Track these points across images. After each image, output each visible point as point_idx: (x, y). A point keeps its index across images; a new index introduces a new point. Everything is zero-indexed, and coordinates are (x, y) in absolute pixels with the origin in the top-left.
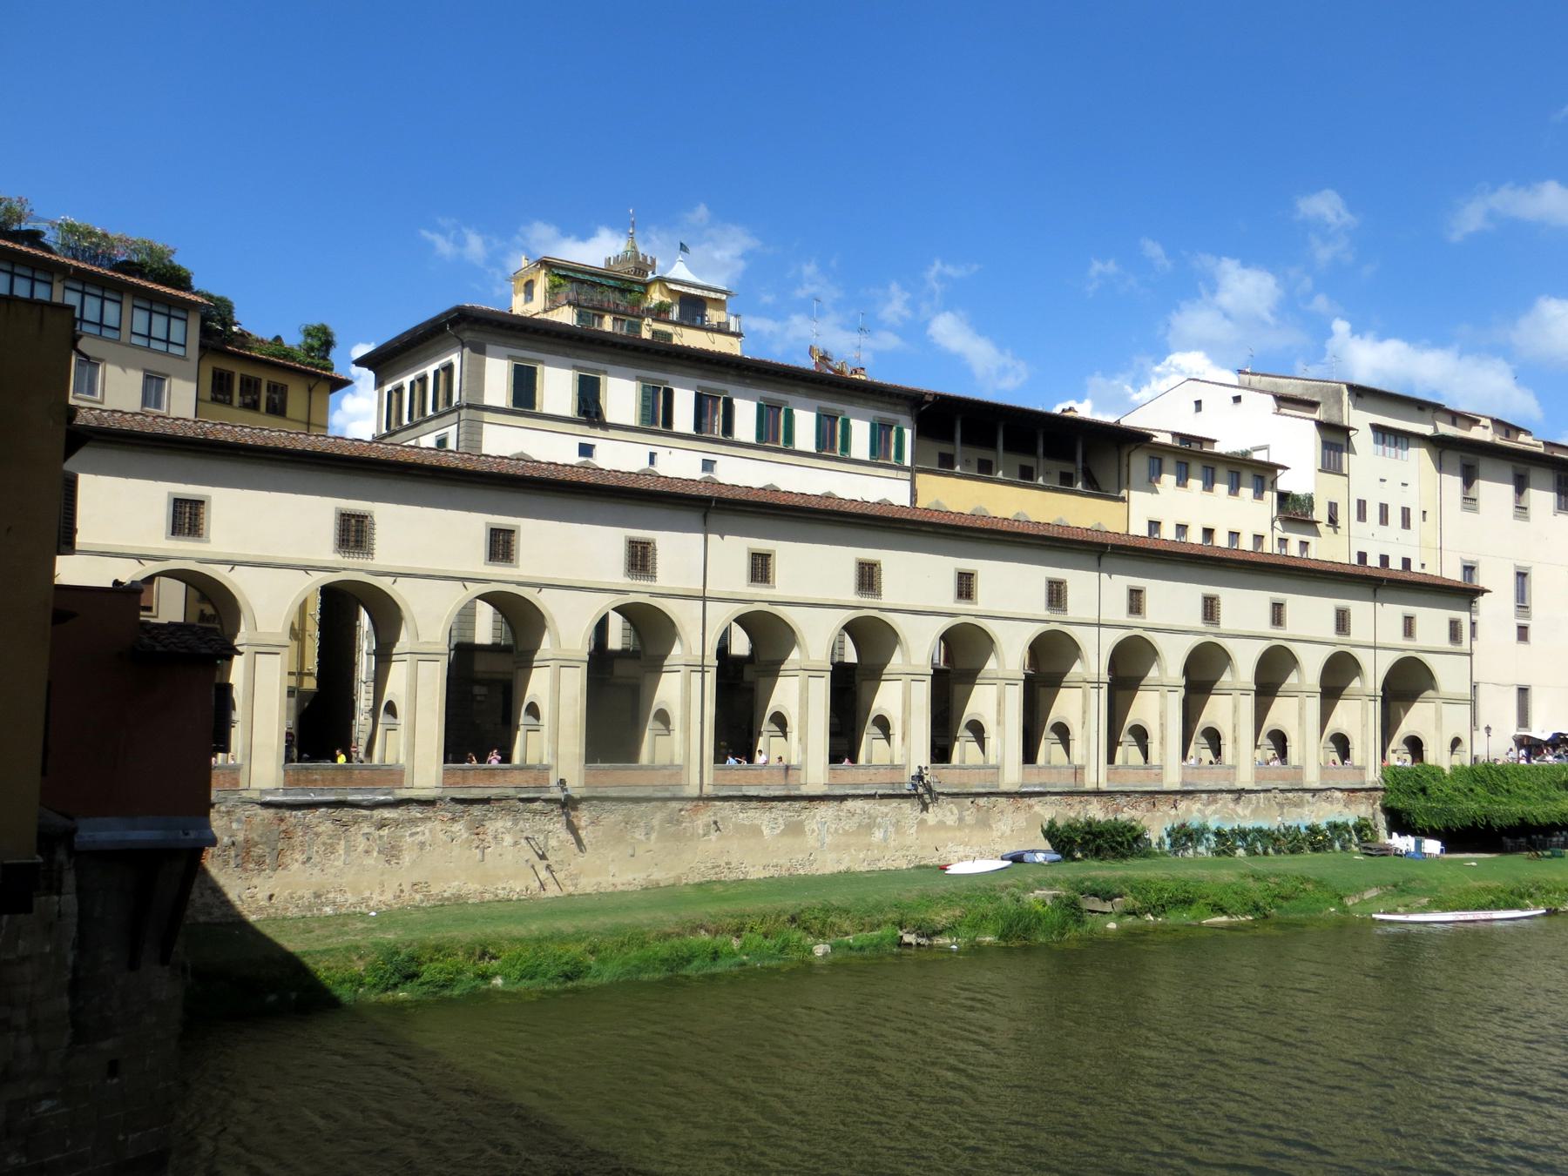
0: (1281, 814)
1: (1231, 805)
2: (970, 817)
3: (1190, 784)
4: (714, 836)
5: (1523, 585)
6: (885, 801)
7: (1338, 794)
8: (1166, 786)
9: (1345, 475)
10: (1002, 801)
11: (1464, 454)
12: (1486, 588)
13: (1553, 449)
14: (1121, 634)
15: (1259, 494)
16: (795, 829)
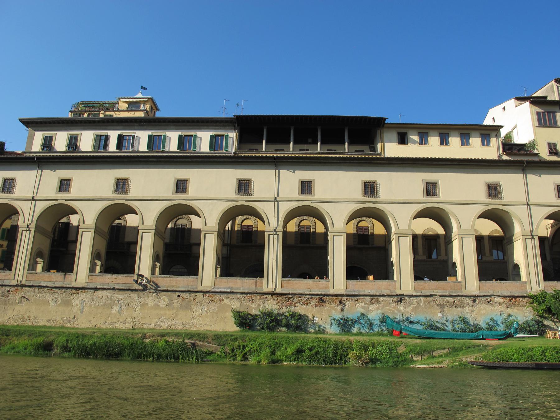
2: (176, 304)
3: (354, 291)
4: (25, 302)
6: (121, 292)
10: (200, 295)
16: (68, 303)
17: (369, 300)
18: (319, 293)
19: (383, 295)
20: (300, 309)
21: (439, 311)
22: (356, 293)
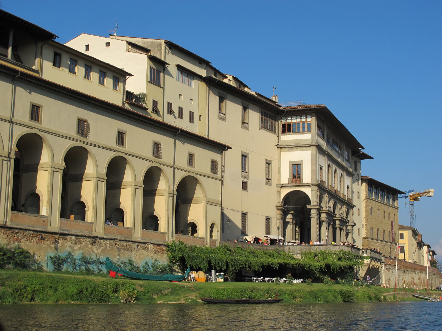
0: (119, 255)
1: (90, 246)
3: (65, 230)
5: (245, 161)
7: (151, 246)
8: (49, 229)
9: (162, 88)
11: (221, 91)
12: (230, 146)
14: (25, 131)
15: (115, 88)
17: (75, 239)
18: (41, 229)
19: (85, 236)
20: (25, 245)
21: (117, 254)
22: (66, 232)
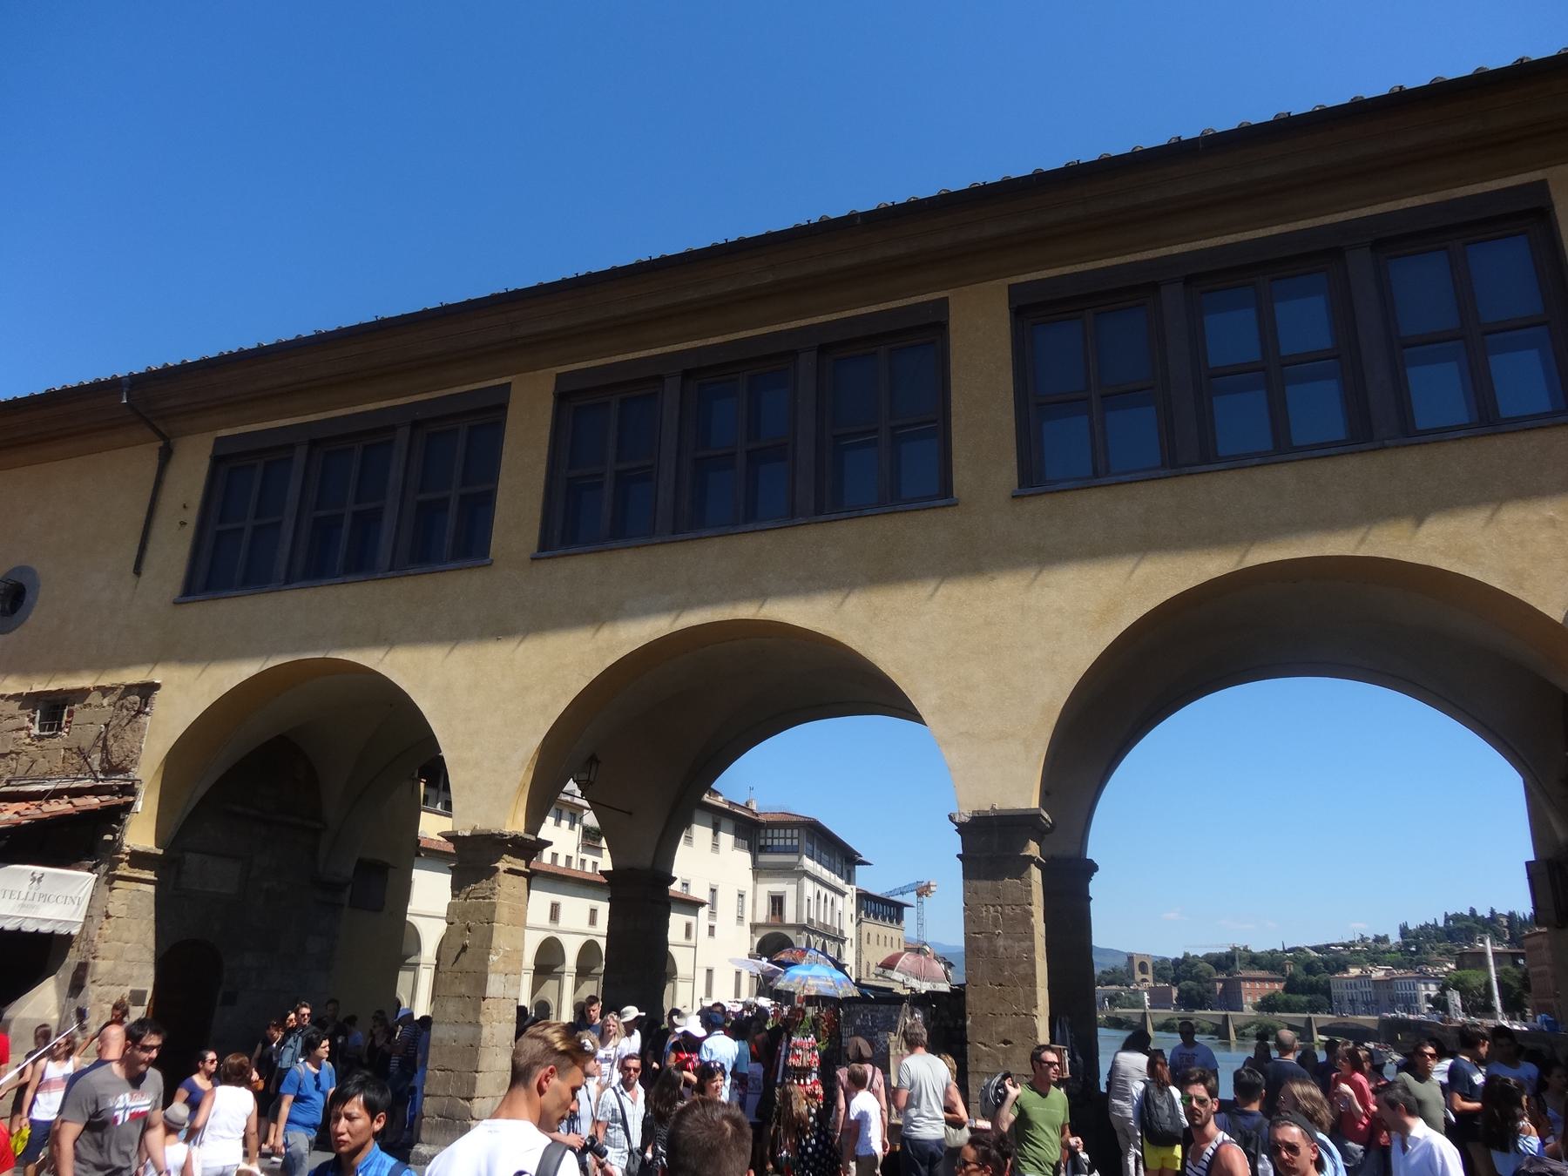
13: (735, 807)
15: (572, 827)
